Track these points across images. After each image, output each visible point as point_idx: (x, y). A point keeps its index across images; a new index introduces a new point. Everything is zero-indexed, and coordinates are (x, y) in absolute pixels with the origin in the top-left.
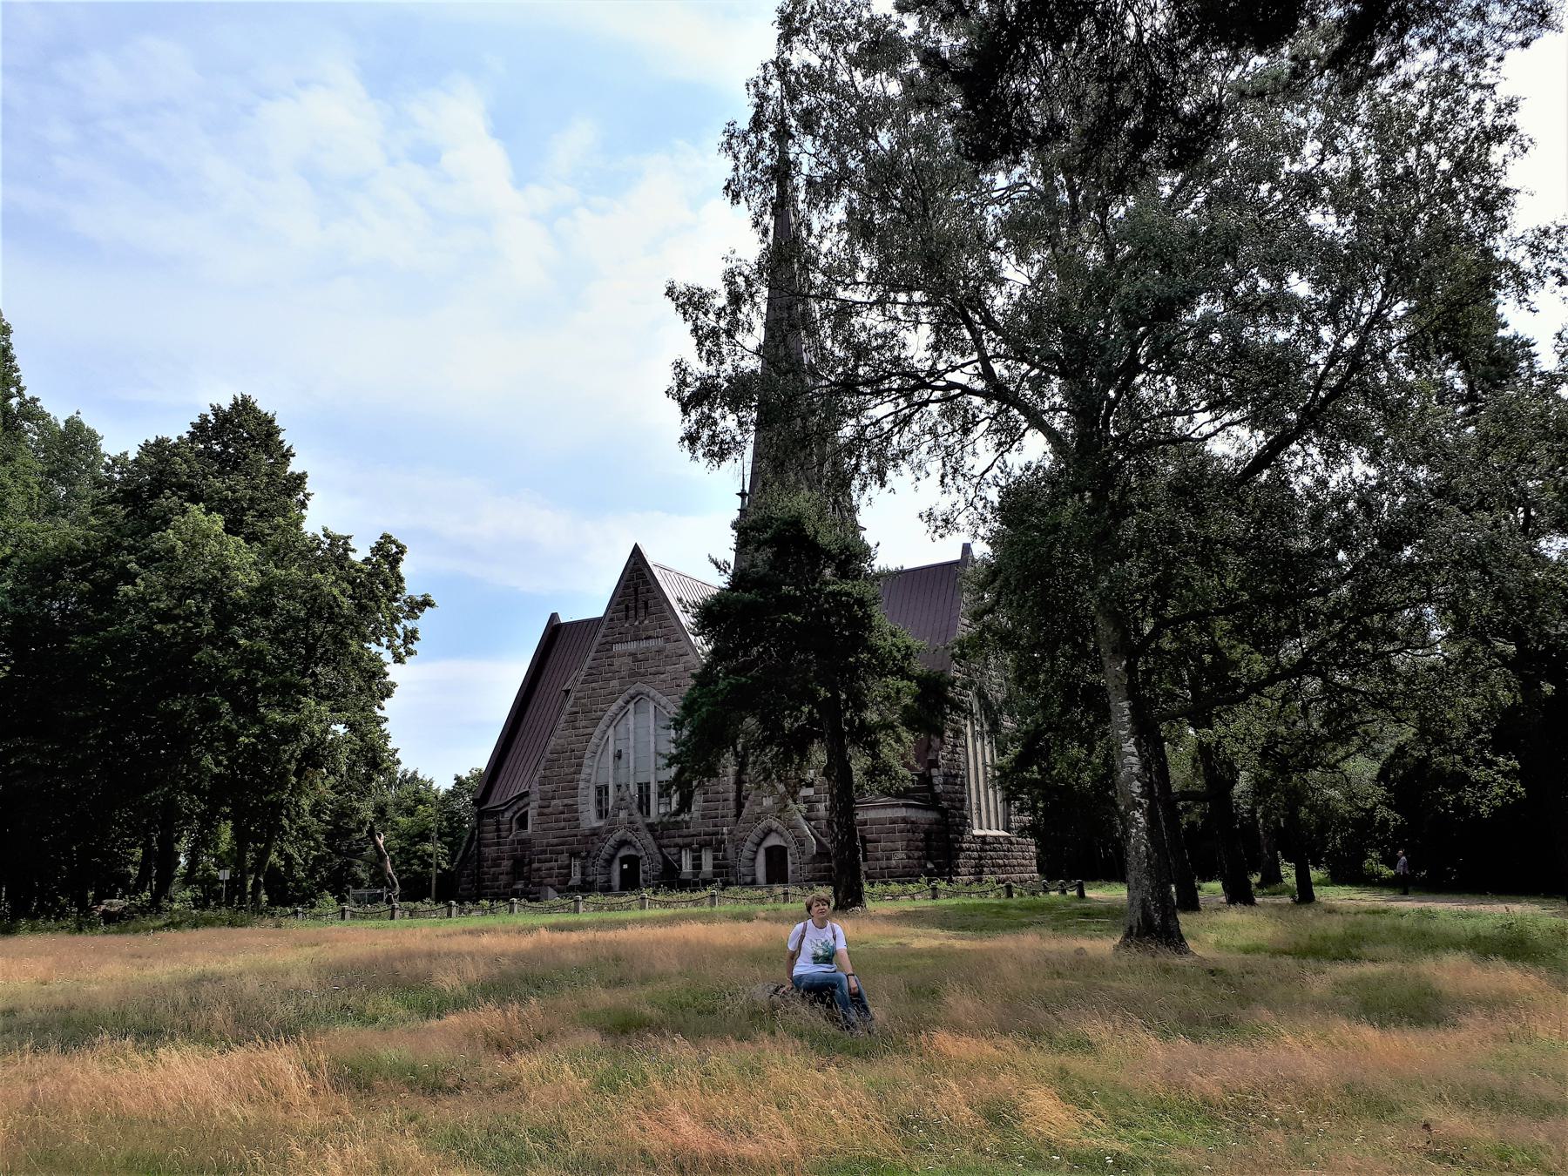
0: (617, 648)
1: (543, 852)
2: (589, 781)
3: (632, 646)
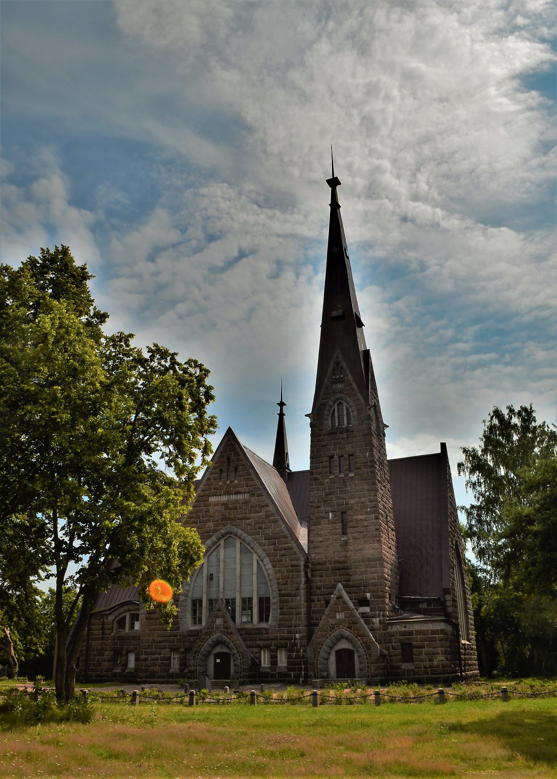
3: (225, 498)
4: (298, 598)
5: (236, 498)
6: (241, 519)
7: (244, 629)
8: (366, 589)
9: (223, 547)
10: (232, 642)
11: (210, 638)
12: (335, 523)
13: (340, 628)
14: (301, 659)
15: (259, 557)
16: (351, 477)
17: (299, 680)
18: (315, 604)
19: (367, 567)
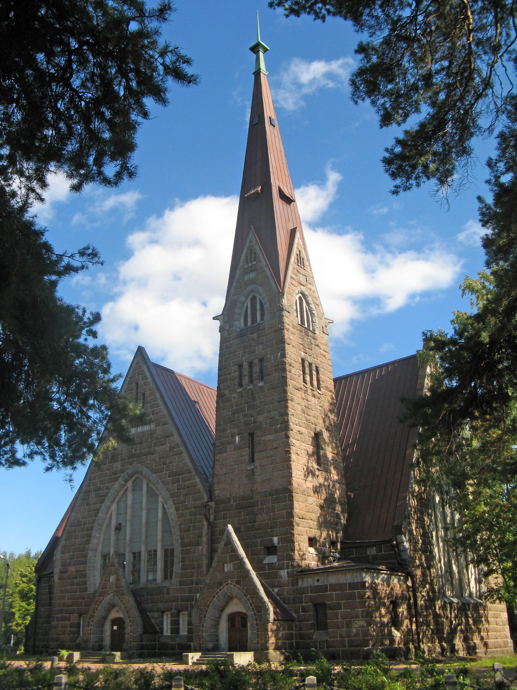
1: (61, 611)
2: (96, 550)
4: (200, 547)
6: (146, 455)
7: (145, 588)
10: (124, 604)
11: (103, 599)
16: (261, 387)
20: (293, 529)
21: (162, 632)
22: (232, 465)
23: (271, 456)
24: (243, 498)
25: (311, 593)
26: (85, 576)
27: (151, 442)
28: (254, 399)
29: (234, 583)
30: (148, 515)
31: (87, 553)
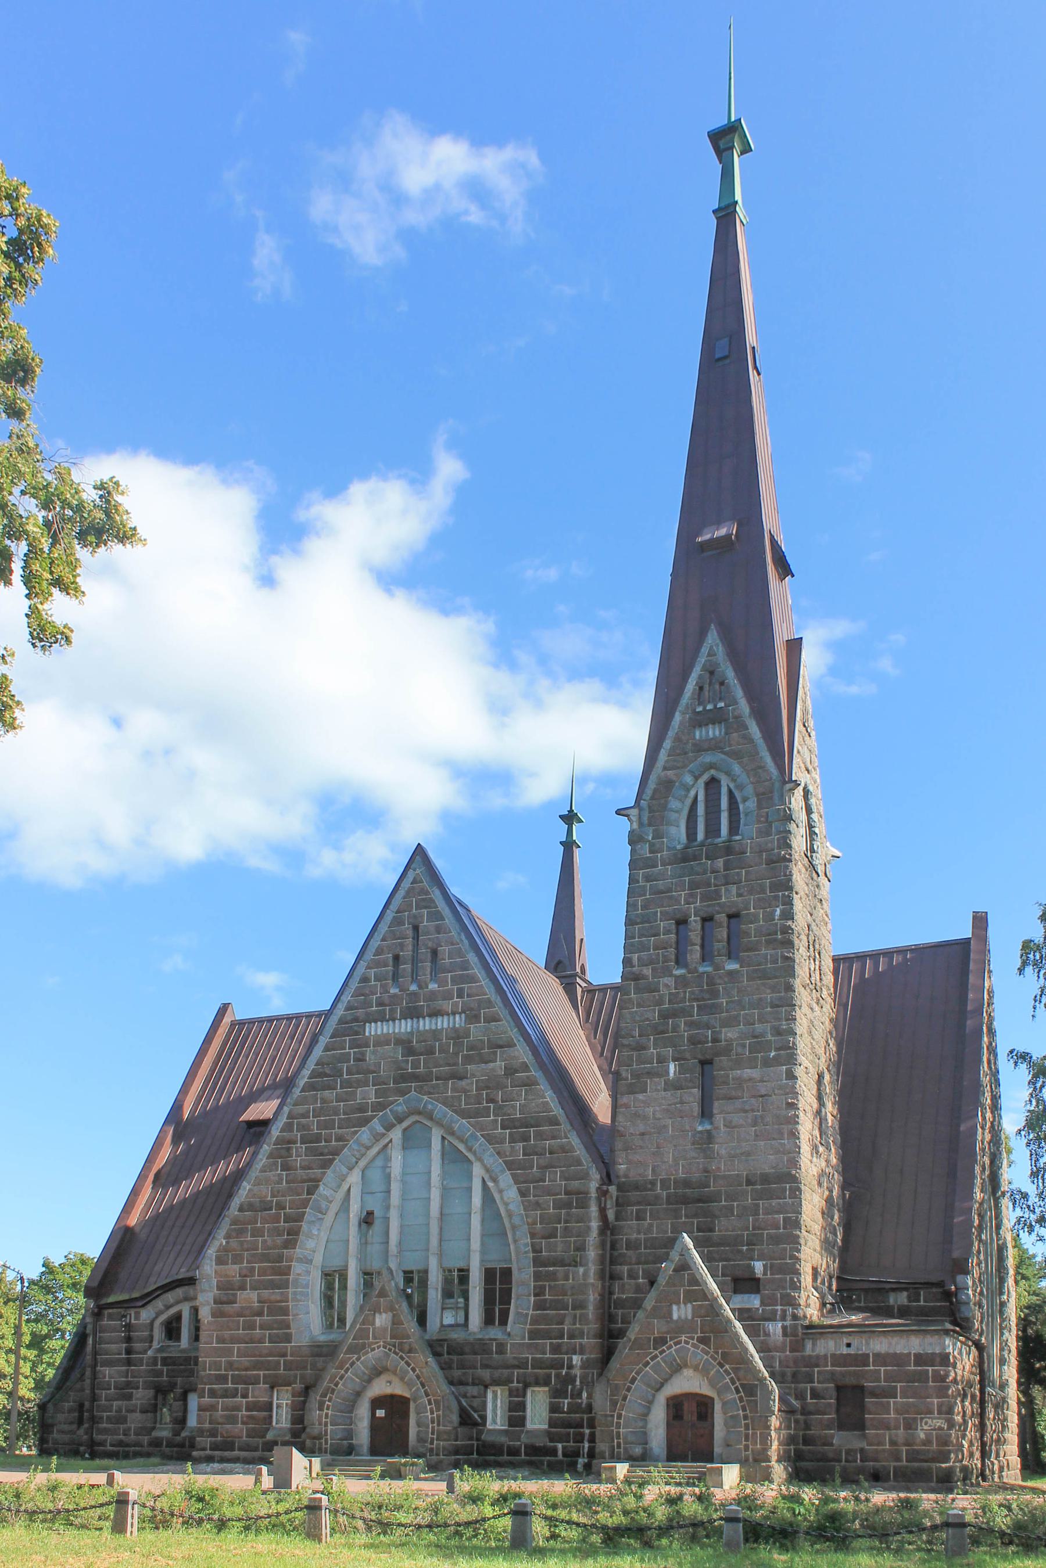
0: (373, 1030)
3: (404, 1027)
4: (581, 1270)
5: (434, 1027)
7: (445, 1340)
8: (753, 1250)
9: (400, 1147)
10: (414, 1370)
11: (358, 1359)
12: (681, 1088)
13: (679, 1342)
14: (583, 1413)
15: (487, 1170)
16: (731, 973)
17: (576, 1463)
18: (623, 1285)
19: (759, 1196)
20: (799, 1251)
21: (484, 1424)
22: (659, 1119)
23: (753, 1110)
24: (687, 1183)
25: (832, 1365)
26: (285, 1312)
27: (456, 1054)
28: (715, 994)
29: (695, 1342)
30: (443, 1197)
31: (290, 1267)
